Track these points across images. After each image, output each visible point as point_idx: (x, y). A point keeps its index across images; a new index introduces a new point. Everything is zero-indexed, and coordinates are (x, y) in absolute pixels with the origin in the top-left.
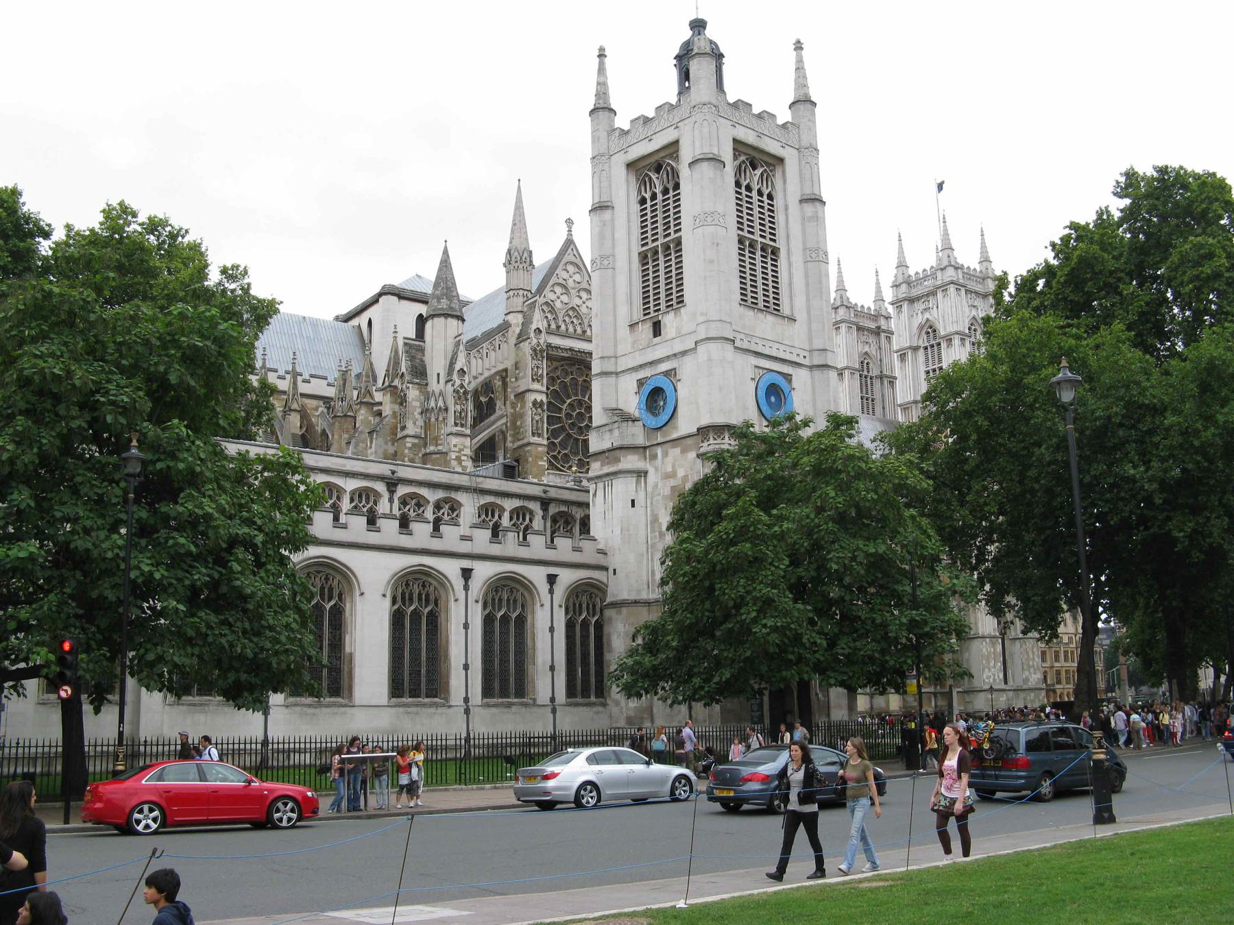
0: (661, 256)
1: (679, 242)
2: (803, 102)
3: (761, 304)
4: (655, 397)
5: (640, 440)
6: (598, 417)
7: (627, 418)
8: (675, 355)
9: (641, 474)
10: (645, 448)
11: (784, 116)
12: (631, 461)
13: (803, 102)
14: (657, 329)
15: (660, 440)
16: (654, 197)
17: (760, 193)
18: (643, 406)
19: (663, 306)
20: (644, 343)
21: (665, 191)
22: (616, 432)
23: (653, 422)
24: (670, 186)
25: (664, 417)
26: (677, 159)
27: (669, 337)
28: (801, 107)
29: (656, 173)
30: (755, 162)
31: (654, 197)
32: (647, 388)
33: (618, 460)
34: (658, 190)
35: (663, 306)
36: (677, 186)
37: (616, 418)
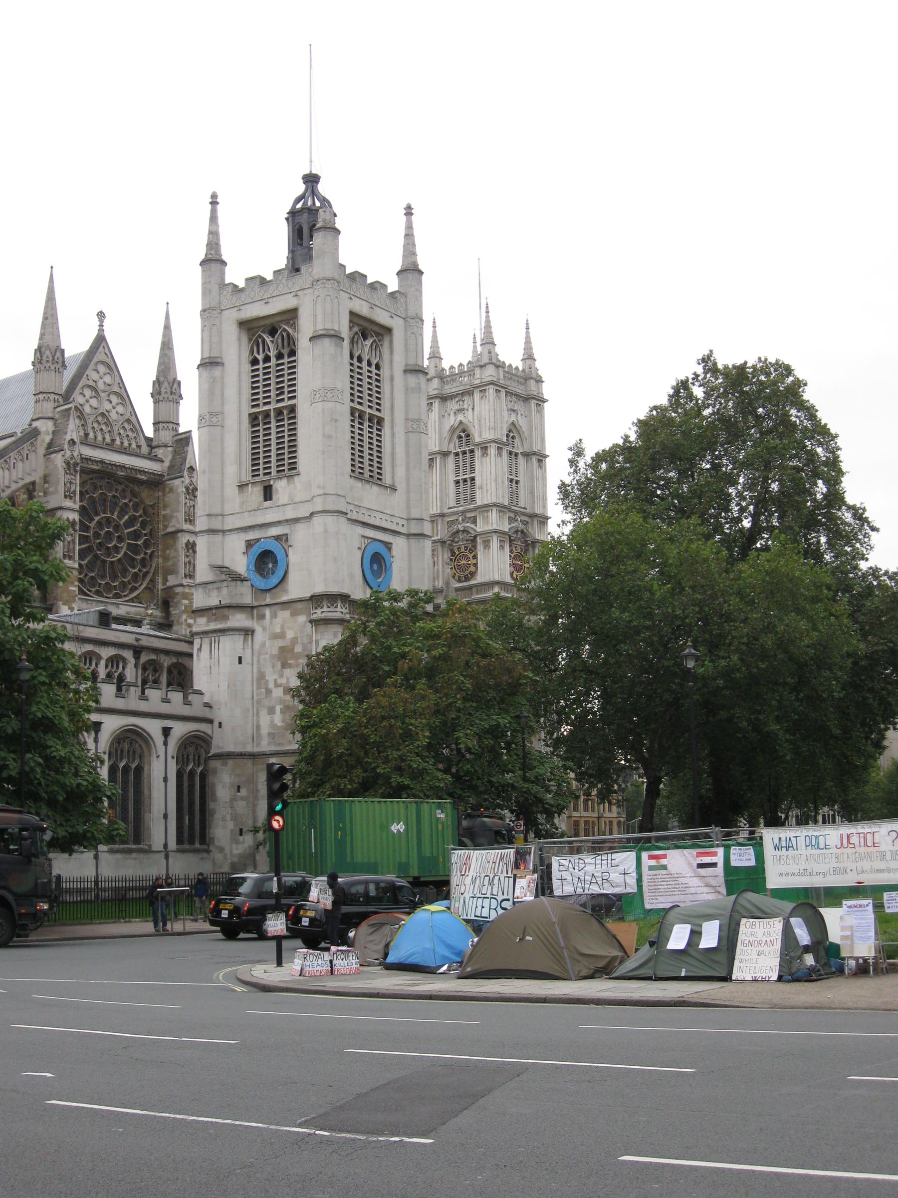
0: (273, 424)
1: (292, 409)
2: (411, 271)
3: (367, 474)
4: (265, 560)
5: (248, 600)
6: (203, 573)
7: (236, 578)
8: (287, 521)
9: (248, 633)
10: (253, 607)
11: (393, 285)
12: (239, 620)
13: (411, 271)
14: (268, 492)
15: (268, 601)
16: (267, 359)
17: (369, 364)
18: (252, 567)
19: (273, 470)
20: (255, 506)
21: (280, 356)
22: (225, 591)
23: (261, 583)
24: (285, 352)
25: (274, 580)
26: (294, 326)
27: (281, 502)
28: (410, 275)
29: (270, 337)
30: (367, 331)
31: (267, 359)
32: (257, 550)
33: (226, 618)
34: (272, 354)
35: (273, 470)
36: (293, 353)
37: (223, 577)
